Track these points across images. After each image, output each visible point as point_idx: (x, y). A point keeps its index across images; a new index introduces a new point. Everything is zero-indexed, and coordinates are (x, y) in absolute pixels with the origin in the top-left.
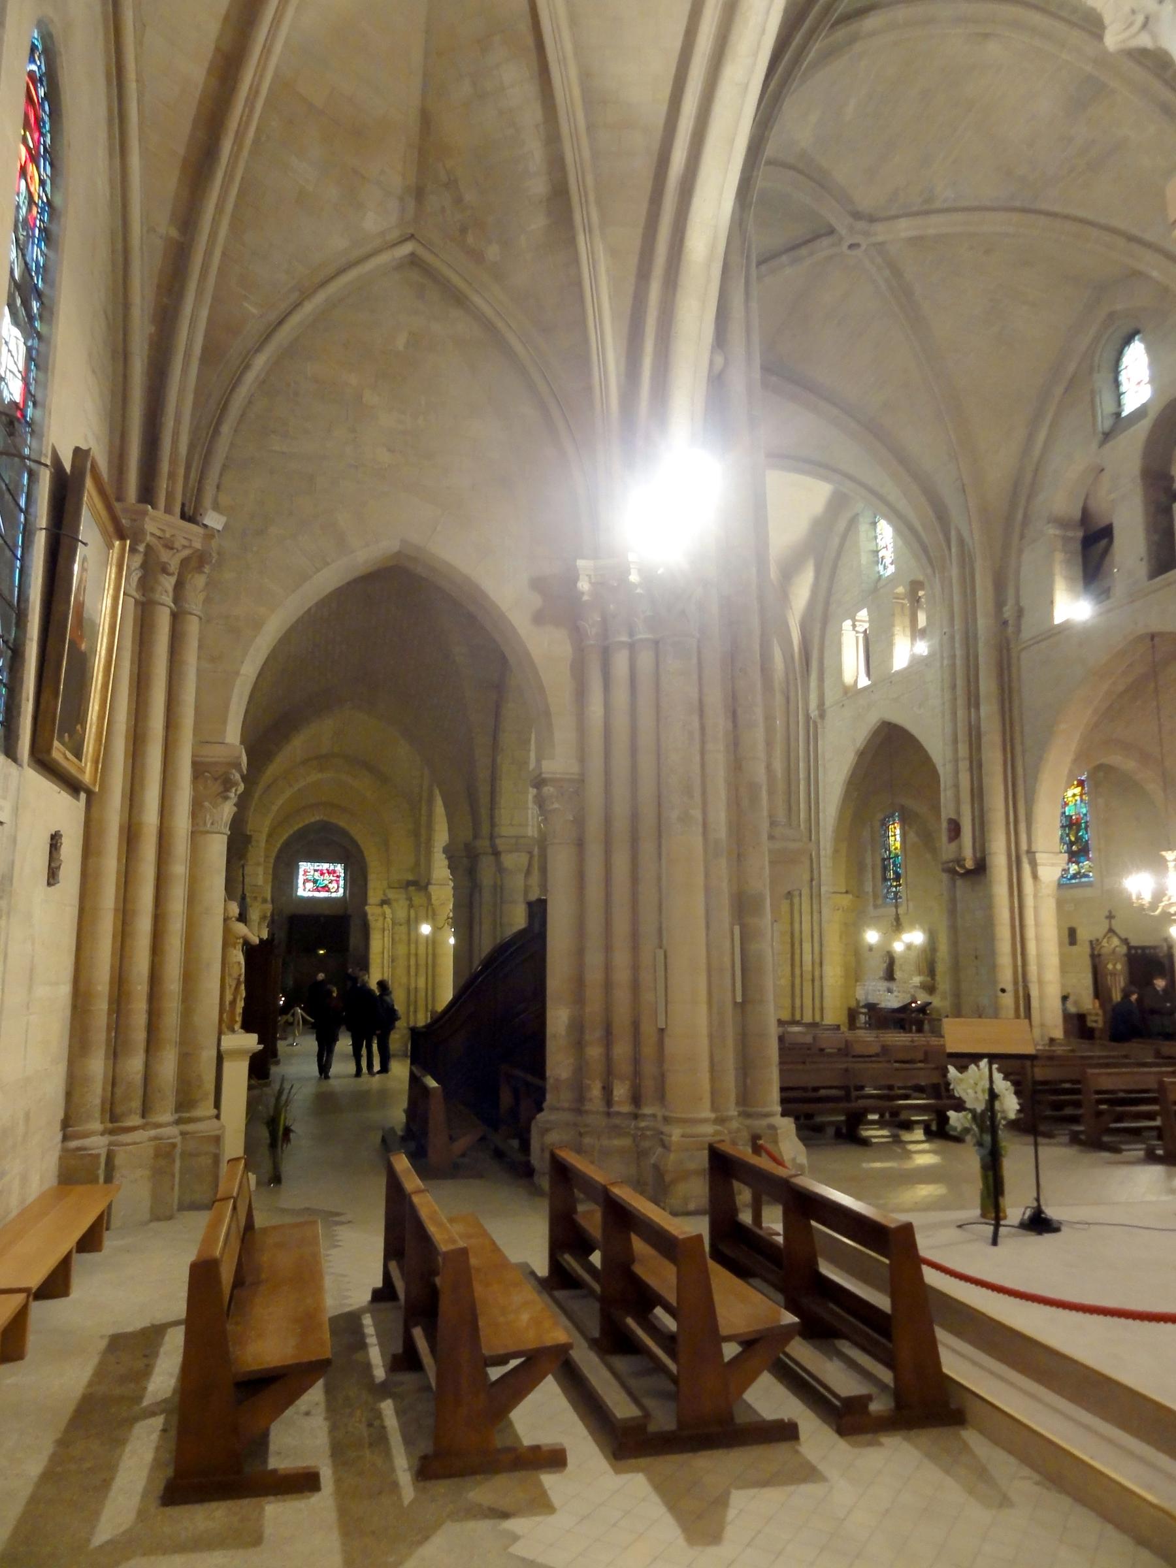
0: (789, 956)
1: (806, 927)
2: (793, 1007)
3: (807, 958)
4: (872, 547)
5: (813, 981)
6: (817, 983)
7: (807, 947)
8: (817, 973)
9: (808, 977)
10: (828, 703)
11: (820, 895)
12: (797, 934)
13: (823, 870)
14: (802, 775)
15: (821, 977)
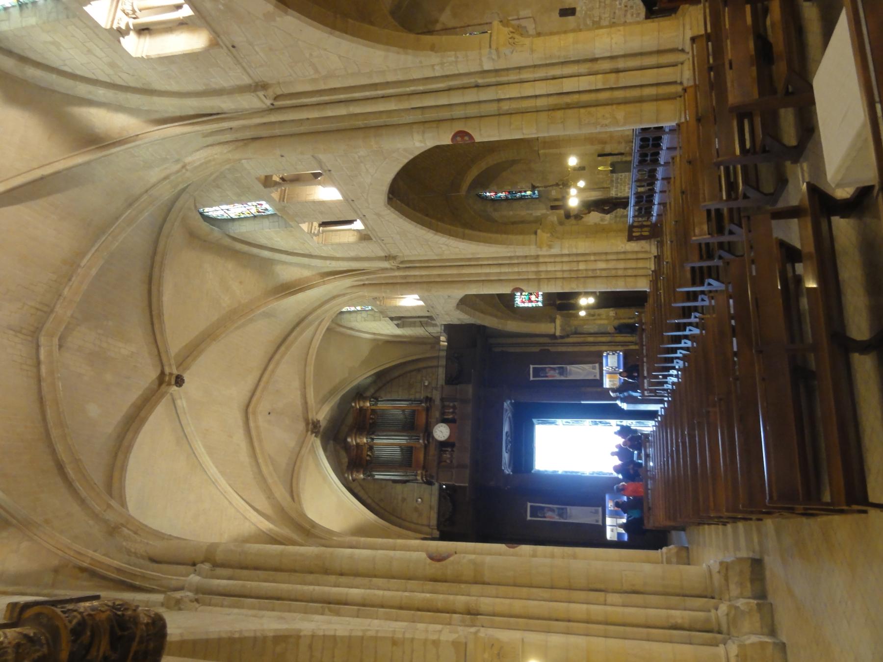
0: (582, 110)
1: (541, 88)
2: (657, 99)
3: (584, 83)
4: (15, 12)
5: (617, 71)
6: (621, 64)
7: (569, 85)
8: (606, 65)
9: (612, 80)
10: (247, 81)
11: (496, 71)
12: (552, 101)
13: (462, 69)
14: (342, 111)
15: (612, 58)
